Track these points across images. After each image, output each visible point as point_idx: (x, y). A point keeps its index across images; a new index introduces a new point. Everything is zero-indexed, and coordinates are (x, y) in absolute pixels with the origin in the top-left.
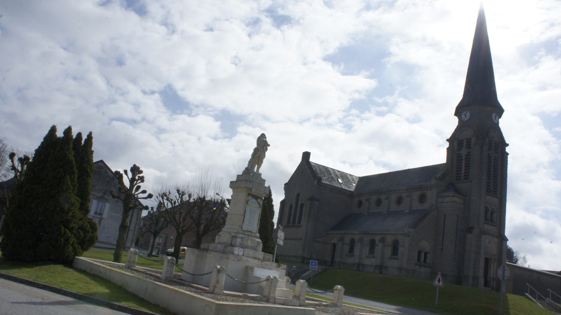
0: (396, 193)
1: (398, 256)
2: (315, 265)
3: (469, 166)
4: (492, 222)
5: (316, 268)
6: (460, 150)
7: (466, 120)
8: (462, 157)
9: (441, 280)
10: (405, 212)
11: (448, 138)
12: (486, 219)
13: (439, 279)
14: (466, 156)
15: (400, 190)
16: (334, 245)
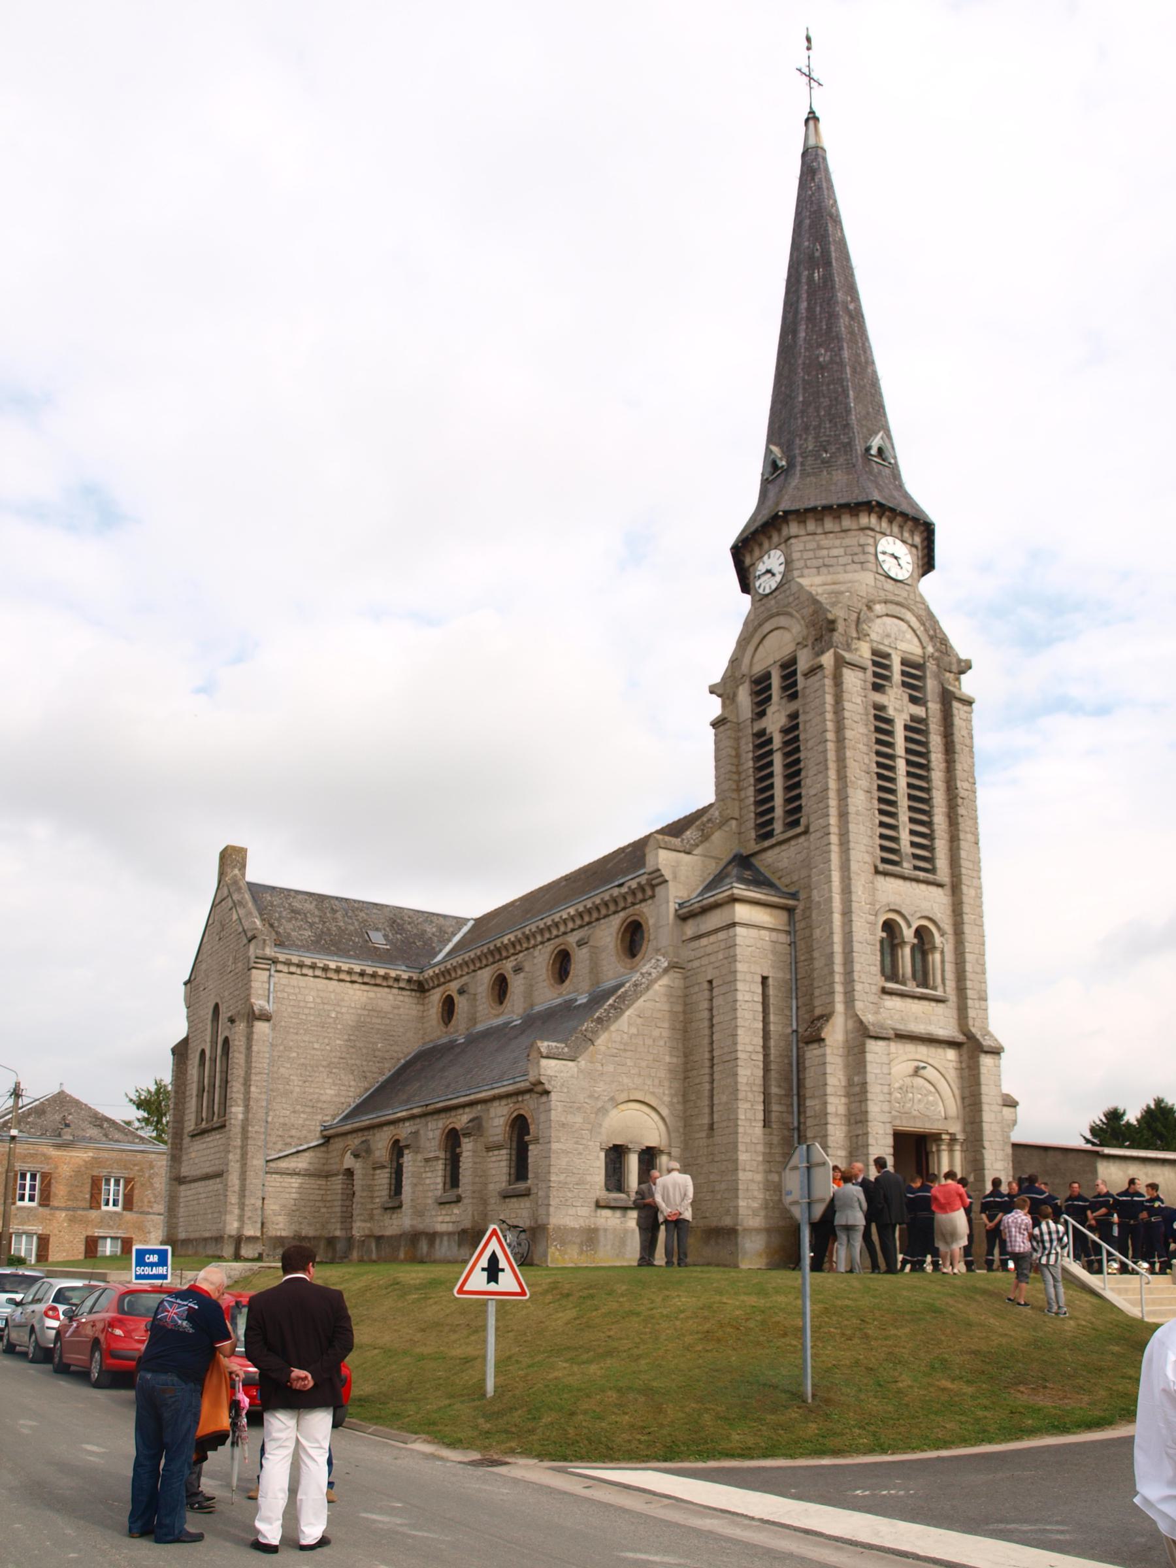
0: (549, 940)
1: (529, 1181)
2: (163, 1262)
3: (798, 772)
4: (924, 984)
5: (164, 1277)
6: (762, 714)
7: (770, 587)
8: (770, 741)
9: (503, 1263)
10: (578, 1003)
11: (717, 678)
12: (891, 972)
13: (493, 1259)
14: (785, 731)
15: (557, 925)
16: (349, 1173)
